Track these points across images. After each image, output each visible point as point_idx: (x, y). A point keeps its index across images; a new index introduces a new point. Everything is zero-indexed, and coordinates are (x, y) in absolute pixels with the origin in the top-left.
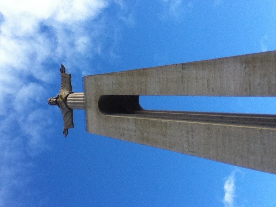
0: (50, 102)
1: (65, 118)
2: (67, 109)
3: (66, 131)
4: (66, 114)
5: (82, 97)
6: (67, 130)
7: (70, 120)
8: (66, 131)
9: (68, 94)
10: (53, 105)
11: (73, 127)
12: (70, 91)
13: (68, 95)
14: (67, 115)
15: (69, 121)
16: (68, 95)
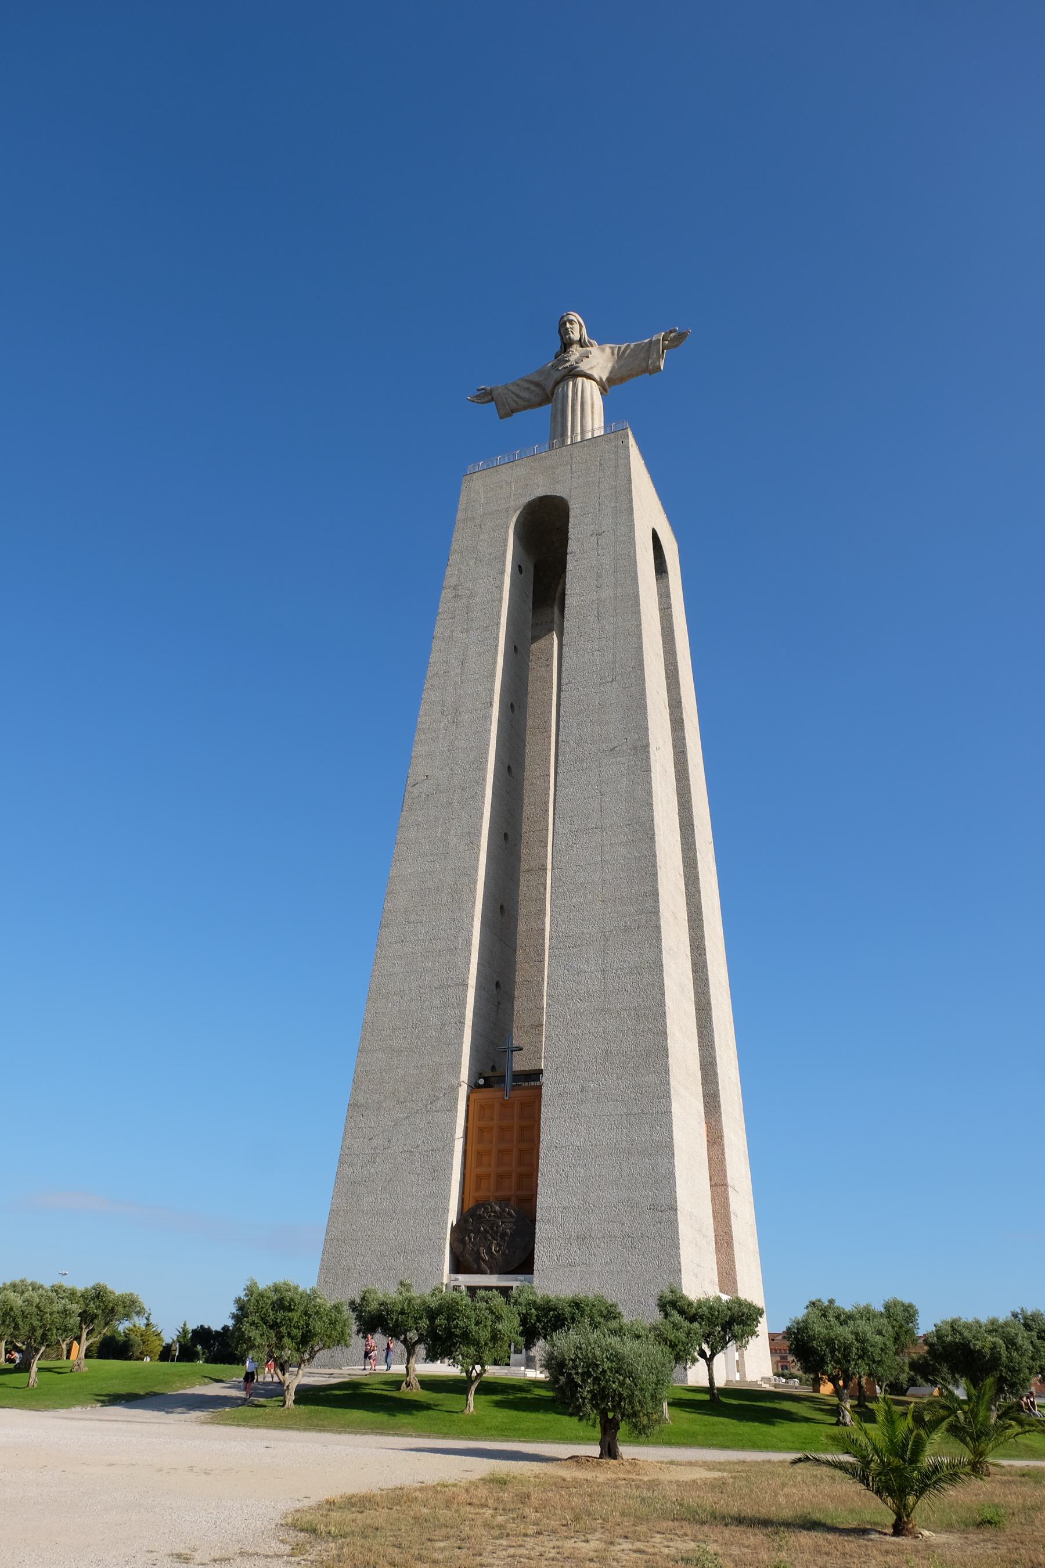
0: (565, 323)
1: (527, 385)
2: (551, 384)
3: (486, 396)
4: (537, 384)
5: (583, 432)
6: (492, 400)
7: (521, 403)
8: (486, 396)
9: (597, 377)
10: (559, 332)
11: (501, 418)
12: (608, 379)
13: (589, 377)
14: (533, 388)
15: (517, 399)
16: (589, 377)
